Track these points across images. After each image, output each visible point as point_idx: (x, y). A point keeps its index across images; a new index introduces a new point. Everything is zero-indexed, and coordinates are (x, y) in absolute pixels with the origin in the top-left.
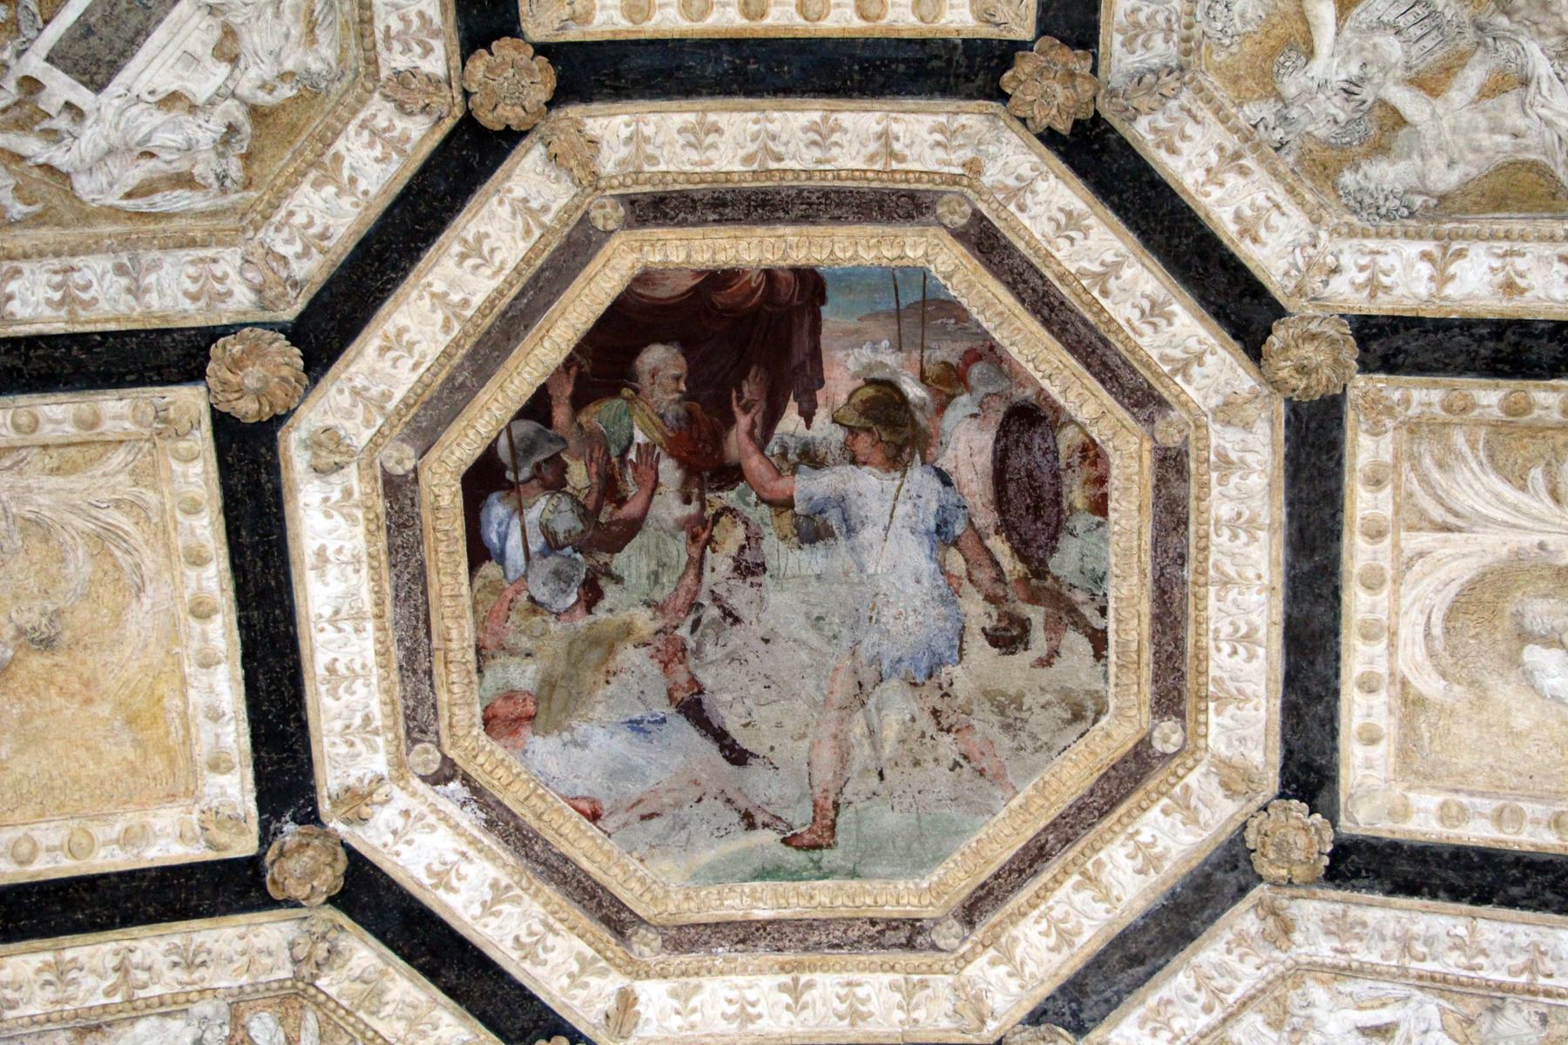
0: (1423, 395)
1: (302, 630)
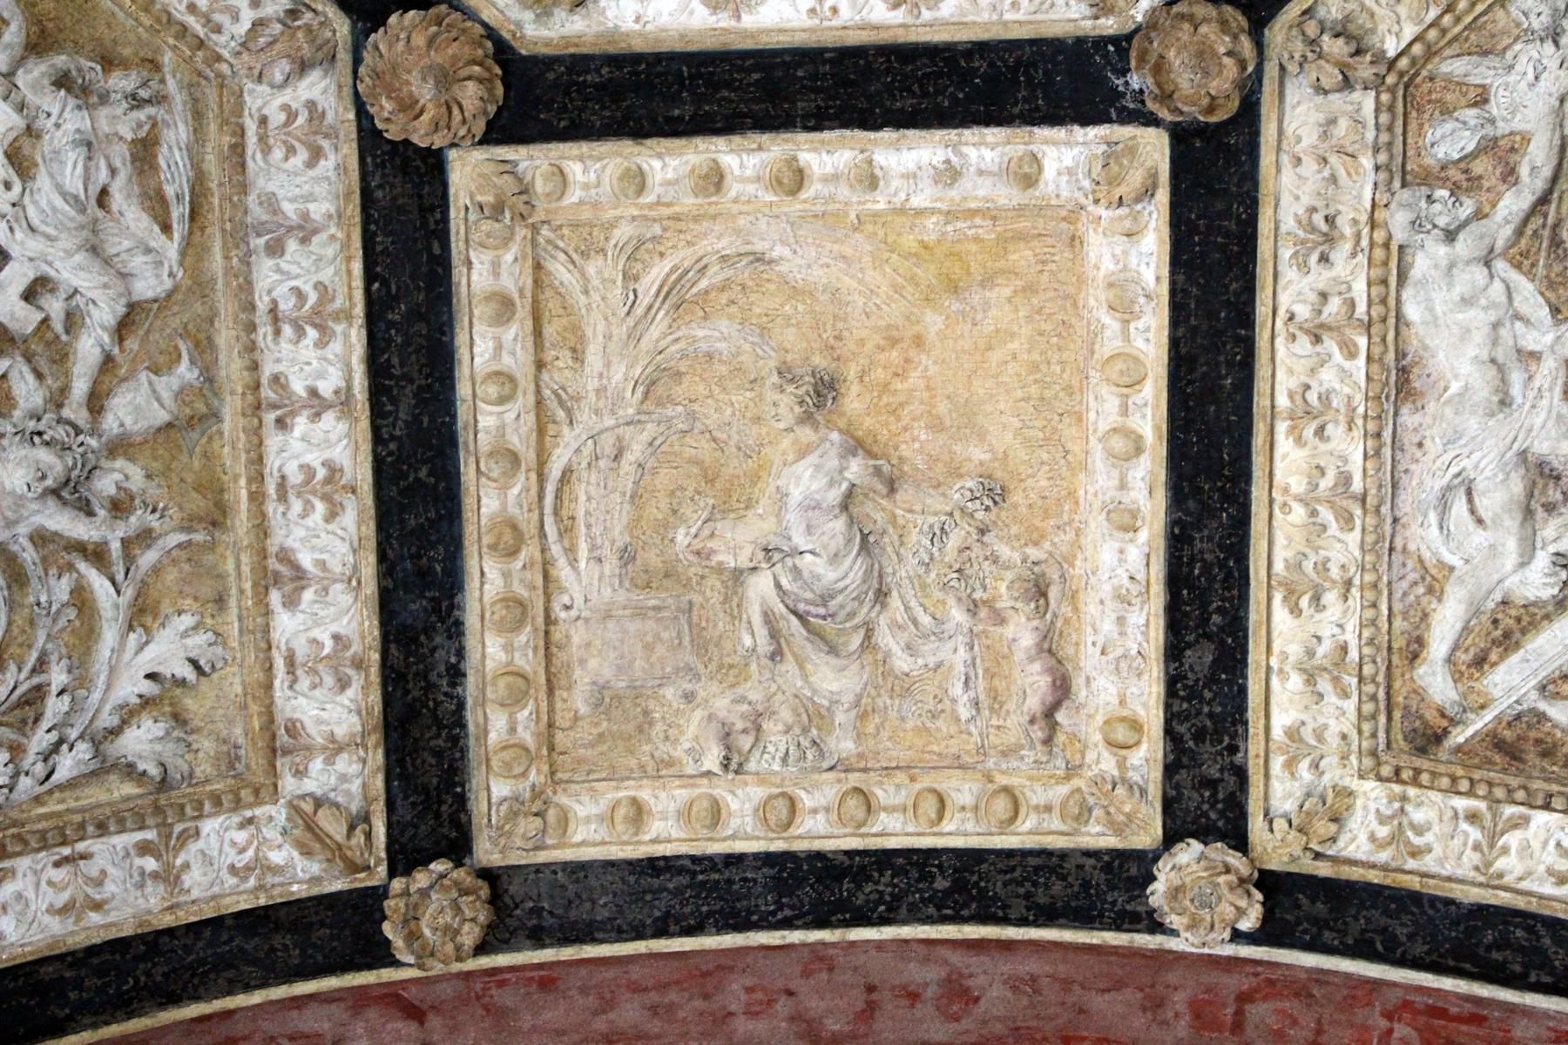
1: (829, 39)
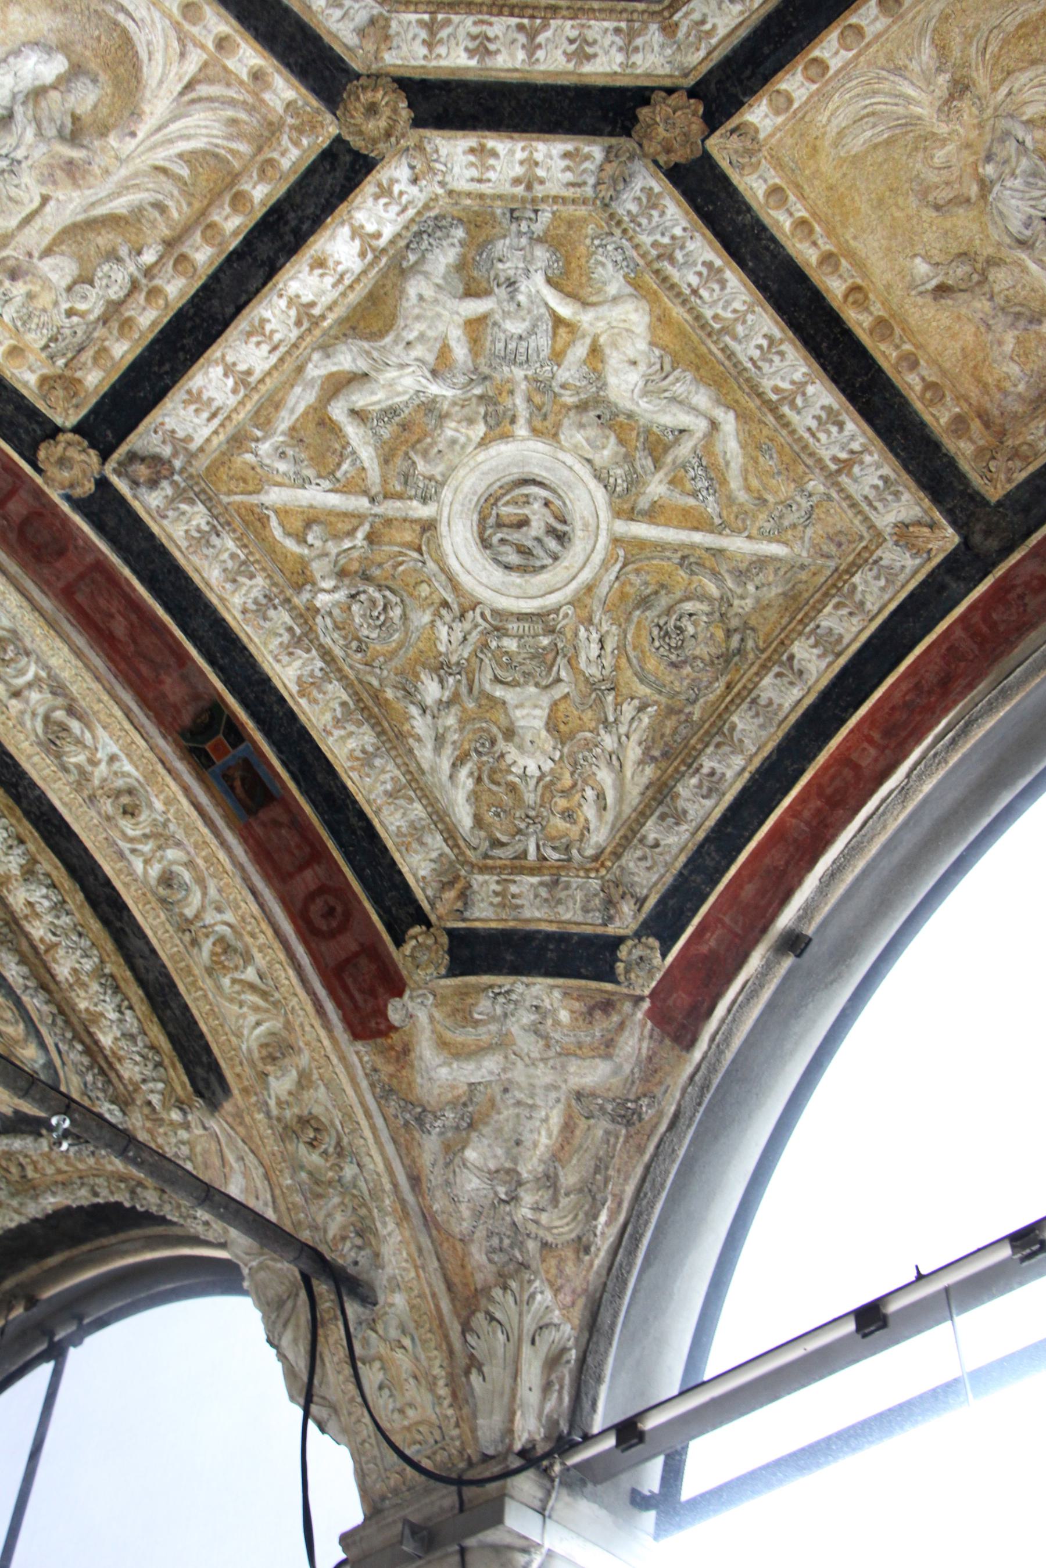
0: (293, 156)
